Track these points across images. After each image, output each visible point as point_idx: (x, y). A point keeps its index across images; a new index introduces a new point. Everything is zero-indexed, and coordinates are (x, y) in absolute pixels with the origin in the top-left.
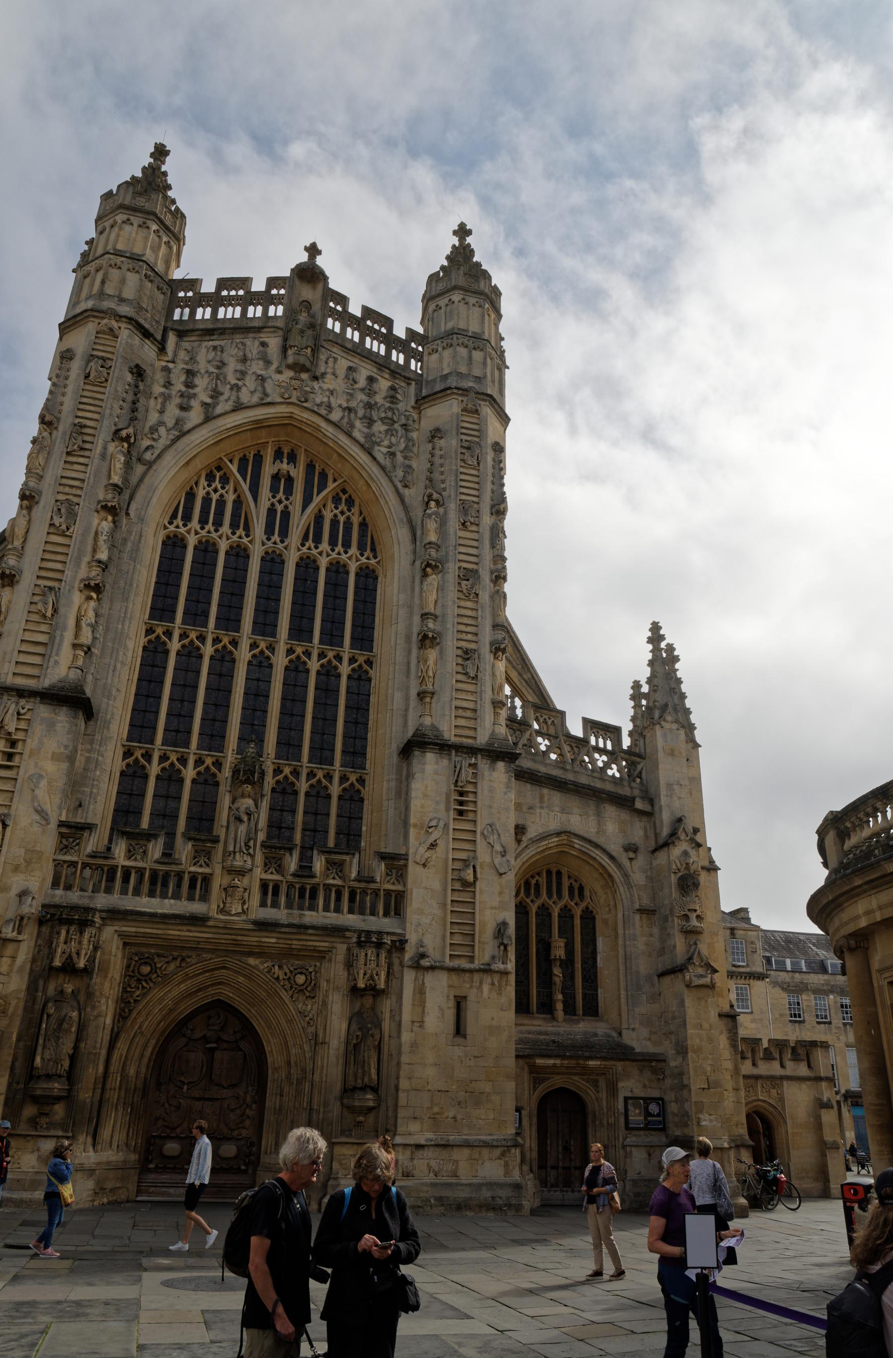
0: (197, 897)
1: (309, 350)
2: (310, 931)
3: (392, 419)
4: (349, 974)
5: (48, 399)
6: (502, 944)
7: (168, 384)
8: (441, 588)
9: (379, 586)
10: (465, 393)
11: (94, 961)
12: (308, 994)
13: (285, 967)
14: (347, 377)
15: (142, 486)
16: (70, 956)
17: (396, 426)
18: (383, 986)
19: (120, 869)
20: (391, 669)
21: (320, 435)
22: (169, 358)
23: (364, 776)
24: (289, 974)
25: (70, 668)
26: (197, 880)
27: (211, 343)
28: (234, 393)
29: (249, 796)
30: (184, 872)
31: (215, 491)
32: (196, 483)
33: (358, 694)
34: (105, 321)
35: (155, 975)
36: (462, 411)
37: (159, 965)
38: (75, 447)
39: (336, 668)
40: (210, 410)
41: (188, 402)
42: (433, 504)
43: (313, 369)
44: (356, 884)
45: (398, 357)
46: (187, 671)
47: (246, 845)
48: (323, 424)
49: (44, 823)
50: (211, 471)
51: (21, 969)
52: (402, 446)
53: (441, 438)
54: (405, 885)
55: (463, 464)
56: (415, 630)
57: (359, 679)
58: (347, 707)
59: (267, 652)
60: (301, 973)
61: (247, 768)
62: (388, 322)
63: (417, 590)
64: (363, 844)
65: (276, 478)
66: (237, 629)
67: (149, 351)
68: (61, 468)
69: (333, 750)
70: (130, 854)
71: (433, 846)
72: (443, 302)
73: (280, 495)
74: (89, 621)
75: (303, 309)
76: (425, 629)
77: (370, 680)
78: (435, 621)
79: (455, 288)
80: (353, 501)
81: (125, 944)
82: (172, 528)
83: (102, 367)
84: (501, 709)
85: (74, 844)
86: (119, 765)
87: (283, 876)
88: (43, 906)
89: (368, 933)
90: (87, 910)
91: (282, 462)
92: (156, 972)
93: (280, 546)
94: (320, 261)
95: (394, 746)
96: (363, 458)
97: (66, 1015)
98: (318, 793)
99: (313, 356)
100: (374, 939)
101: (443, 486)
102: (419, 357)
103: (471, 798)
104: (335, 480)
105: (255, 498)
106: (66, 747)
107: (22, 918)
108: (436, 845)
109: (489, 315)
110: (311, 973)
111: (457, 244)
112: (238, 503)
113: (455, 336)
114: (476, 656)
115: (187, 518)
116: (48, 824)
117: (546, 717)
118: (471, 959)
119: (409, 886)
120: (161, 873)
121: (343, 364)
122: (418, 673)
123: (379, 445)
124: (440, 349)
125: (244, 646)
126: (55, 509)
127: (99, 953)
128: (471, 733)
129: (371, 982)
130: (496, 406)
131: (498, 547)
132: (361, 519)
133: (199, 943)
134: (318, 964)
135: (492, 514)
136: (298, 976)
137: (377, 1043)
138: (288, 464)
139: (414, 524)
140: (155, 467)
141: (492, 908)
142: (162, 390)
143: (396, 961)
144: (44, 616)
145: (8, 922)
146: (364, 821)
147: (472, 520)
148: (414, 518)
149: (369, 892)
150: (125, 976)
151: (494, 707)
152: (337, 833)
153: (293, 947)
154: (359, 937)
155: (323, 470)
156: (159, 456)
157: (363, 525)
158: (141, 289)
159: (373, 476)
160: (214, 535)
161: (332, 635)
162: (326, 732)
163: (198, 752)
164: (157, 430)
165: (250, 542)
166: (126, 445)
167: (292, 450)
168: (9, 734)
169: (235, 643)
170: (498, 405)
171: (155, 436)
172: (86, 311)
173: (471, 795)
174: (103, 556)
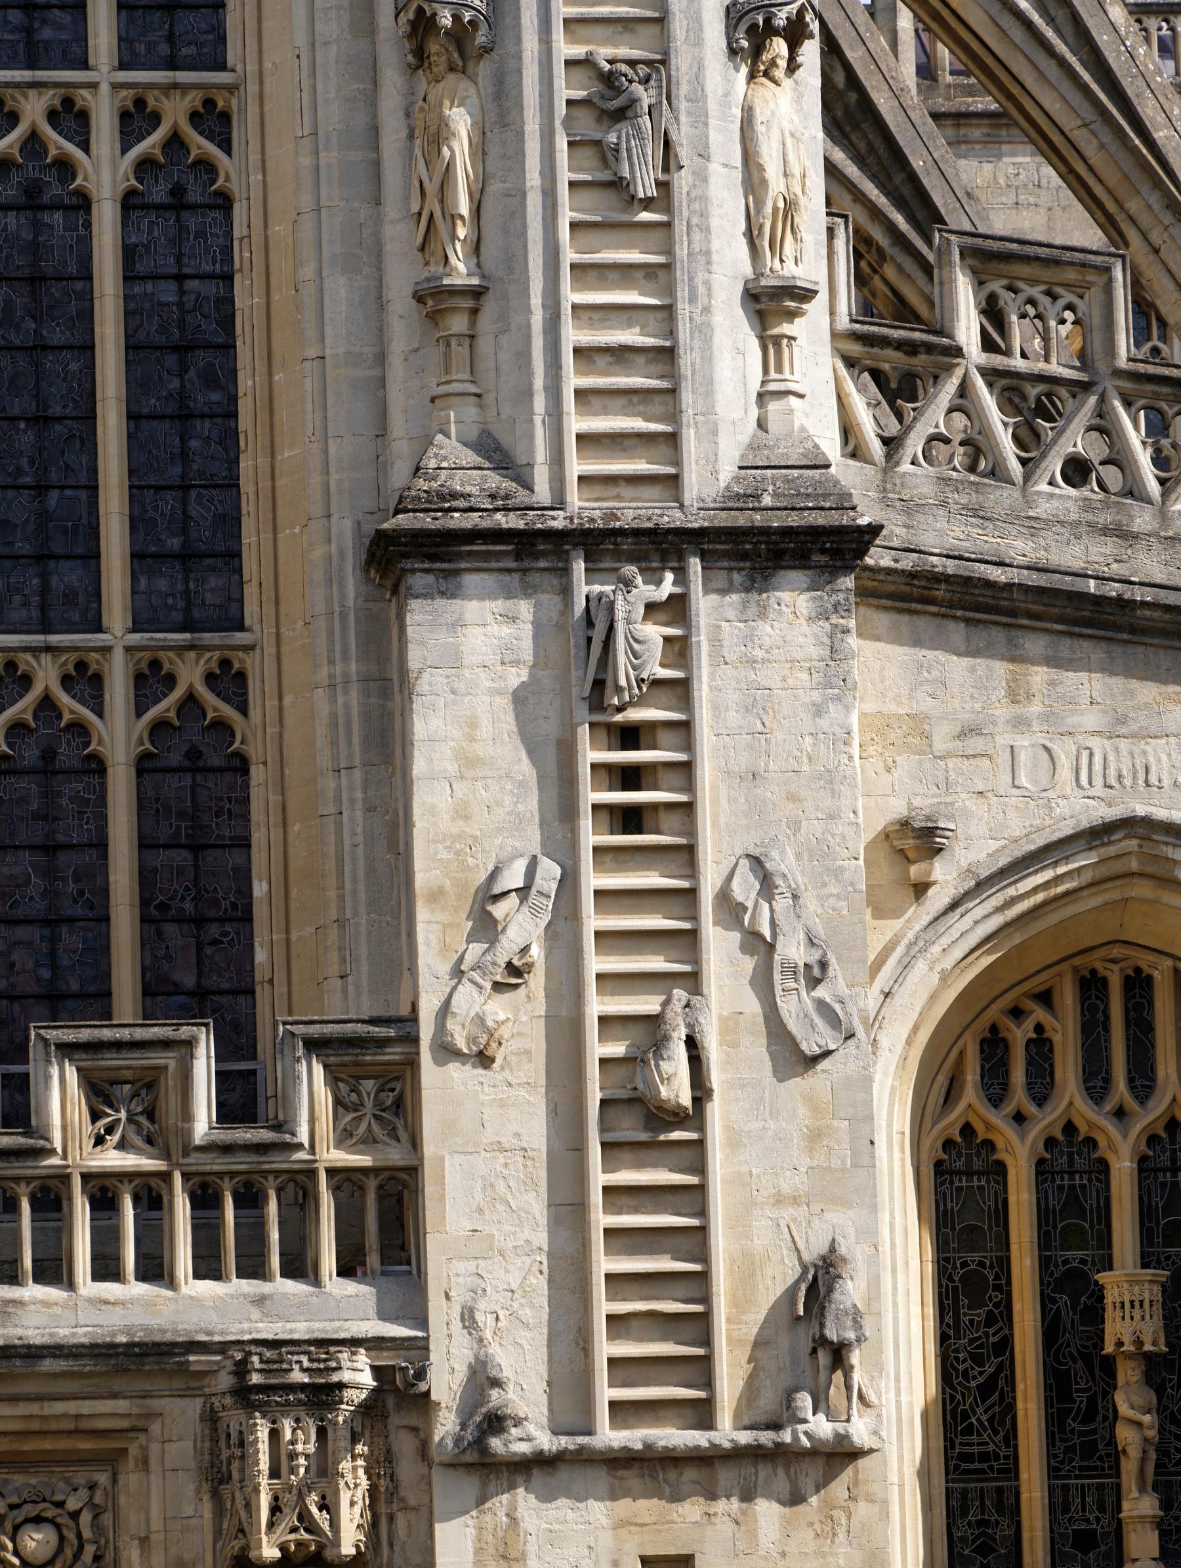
2: (48, 1365)
4: (219, 1511)
6: (823, 1341)
23: (239, 660)
33: (180, 278)
39: (66, 167)
54: (415, 1143)
57: (178, 202)
58: (133, 347)
60: (38, 1520)
64: (260, 956)
69: (94, 555)
77: (225, 202)
84: (792, 315)
95: (344, 527)
98: (49, 755)
110: (75, 1515)
117: (1036, 292)
119: (430, 1148)
122: (407, 198)
134: (103, 1478)
141: (779, 1200)
143: (404, 1444)
152: (145, 920)
162: (54, 476)
173: (663, 736)
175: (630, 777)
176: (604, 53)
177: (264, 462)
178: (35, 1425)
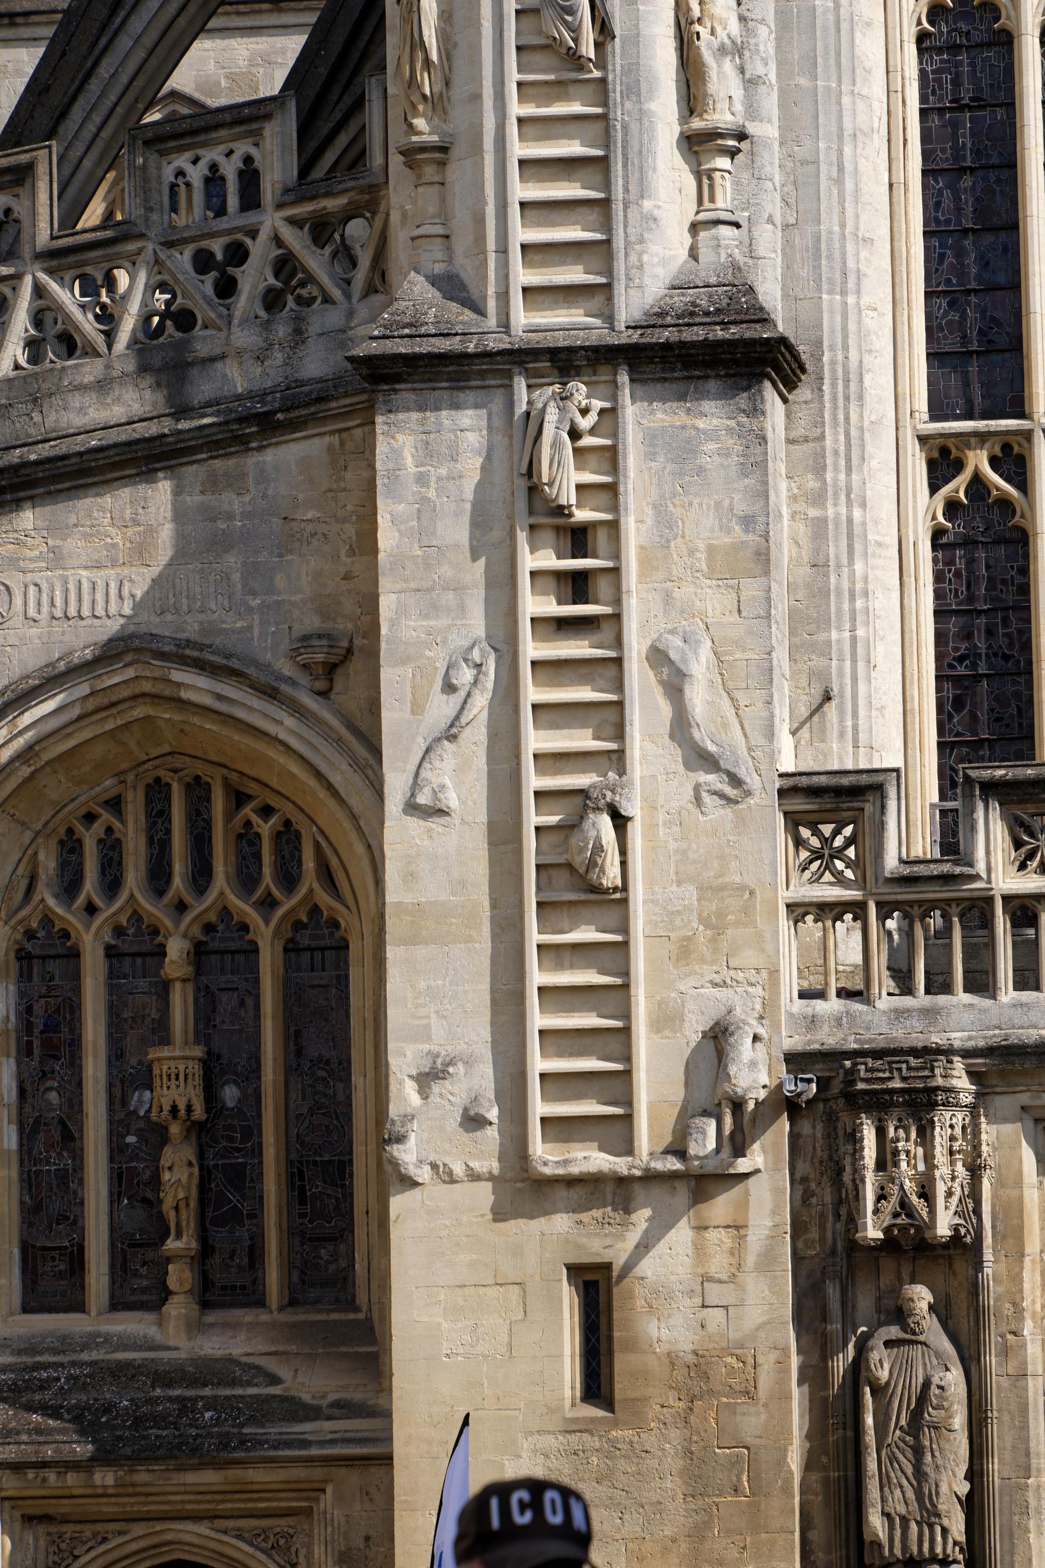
11: (977, 1212)
16: (904, 1204)
51: (767, 1261)
85: (839, 842)
90: (929, 1053)
97: (927, 1384)
106: (747, 522)
116: (748, 793)
168: (561, 511)
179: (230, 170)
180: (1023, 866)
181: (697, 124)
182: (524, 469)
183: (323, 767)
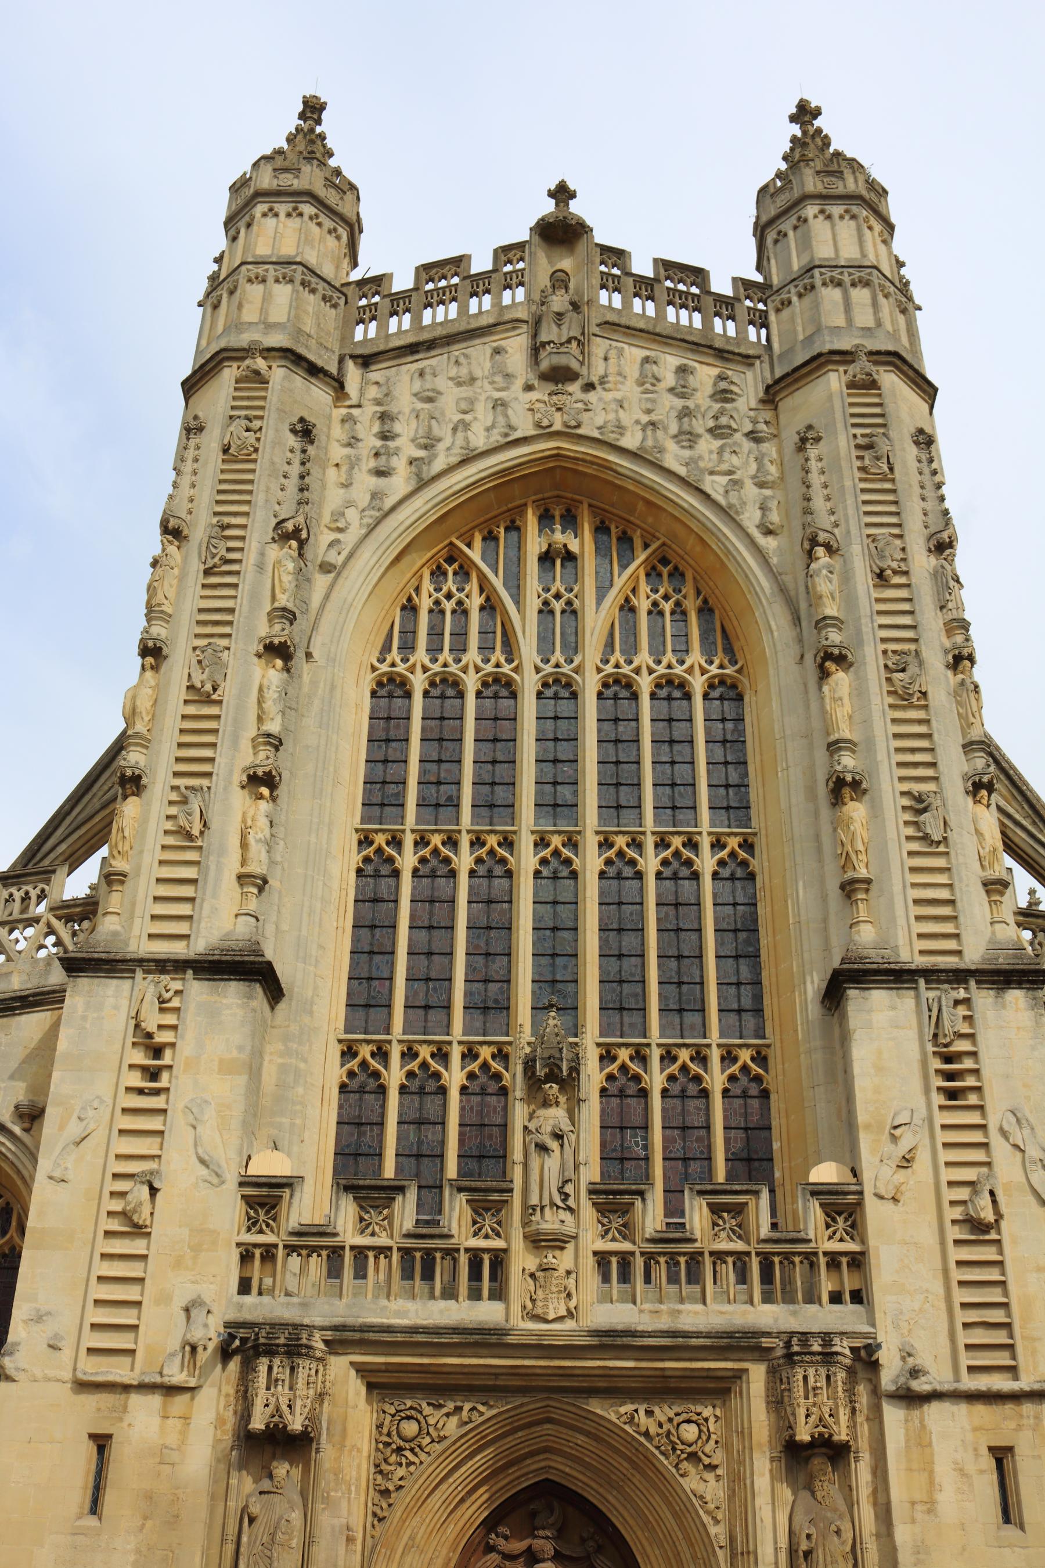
0: (485, 1293)
1: (574, 344)
3: (730, 427)
5: (171, 497)
7: (353, 441)
8: (860, 692)
9: (747, 710)
10: (848, 358)
12: (707, 1461)
13: (656, 1410)
14: (643, 374)
15: (329, 606)
16: (278, 1409)
17: (738, 436)
18: (844, 1437)
19: (348, 1255)
20: (786, 850)
21: (609, 476)
22: (354, 401)
24: (666, 1427)
25: (237, 916)
26: (481, 1262)
27: (416, 366)
28: (460, 435)
29: (557, 1104)
30: (458, 1250)
31: (449, 596)
32: (417, 589)
34: (248, 362)
35: (428, 1440)
36: (851, 385)
37: (432, 1421)
38: (216, 560)
40: (425, 468)
41: (388, 461)
42: (820, 551)
43: (584, 371)
44: (769, 1248)
45: (724, 328)
46: (432, 901)
47: (560, 1190)
48: (613, 458)
49: (215, 1181)
50: (439, 567)
52: (754, 466)
53: (818, 440)
55: (864, 476)
56: (821, 776)
59: (566, 852)
60: (688, 1421)
61: (546, 1055)
62: (698, 275)
63: (814, 706)
65: (546, 558)
66: (513, 819)
67: (319, 395)
68: (197, 597)
70: (364, 1226)
71: (906, 1162)
72: (787, 225)
73: (558, 586)
74: (260, 836)
75: (557, 285)
76: (839, 768)
77: (751, 877)
78: (854, 752)
79: (805, 198)
80: (682, 575)
81: (371, 1387)
82: (384, 668)
83: (248, 430)
86: (335, 1073)
87: (634, 1243)
88: (227, 1325)
89: (805, 1337)
91: (553, 531)
92: (428, 1433)
93: (566, 669)
94: (575, 207)
96: (689, 499)
97: (280, 1518)
99: (582, 353)
100: (816, 1348)
101: (832, 518)
102: (762, 321)
103: (968, 1064)
104: (646, 546)
105: (517, 603)
106: (240, 1048)
107: (194, 1349)
108: (913, 1158)
109: (870, 228)
111: (799, 134)
112: (490, 606)
113: (816, 272)
114: (939, 803)
115: (408, 647)
116: (223, 1182)
118: (1012, 1370)
119: (872, 1241)
120: (418, 1255)
121: (634, 354)
123: (712, 473)
124: (795, 299)
125: (523, 848)
126: (194, 661)
127: (326, 1404)
128: (951, 945)
129: (821, 1429)
130: (905, 368)
131: (950, 605)
132: (699, 602)
133: (496, 1375)
134: (718, 1402)
135: (930, 551)
136: (684, 1426)
137: (848, 1548)
138: (563, 533)
139: (792, 593)
140: (345, 574)
142: (347, 451)
144: (189, 836)
145: (173, 1355)
146: (775, 1132)
147: (894, 565)
148: (791, 586)
149: (797, 1259)
150: (377, 1442)
151: (987, 892)
153: (668, 1373)
154: (788, 1345)
155: (624, 532)
156: (351, 556)
157: (706, 610)
158: (296, 305)
159: (709, 525)
160: (454, 668)
161: (674, 808)
163: (465, 1038)
164: (343, 514)
165: (516, 670)
166: (294, 544)
167: (568, 510)
168: (149, 1036)
169: (508, 843)
170: (911, 367)
171: (340, 525)
172: (217, 353)
174: (273, 727)
175: (950, 1076)
176: (916, 787)
177: (773, 970)
178: (688, 1373)
179: (34, 894)
180: (362, 1232)
181: (243, 870)
182: (133, 1014)
183: (20, 1167)
